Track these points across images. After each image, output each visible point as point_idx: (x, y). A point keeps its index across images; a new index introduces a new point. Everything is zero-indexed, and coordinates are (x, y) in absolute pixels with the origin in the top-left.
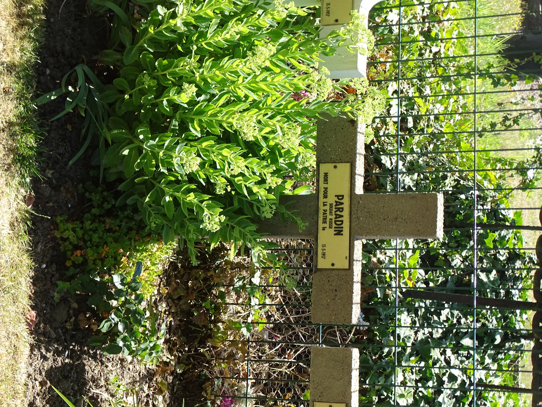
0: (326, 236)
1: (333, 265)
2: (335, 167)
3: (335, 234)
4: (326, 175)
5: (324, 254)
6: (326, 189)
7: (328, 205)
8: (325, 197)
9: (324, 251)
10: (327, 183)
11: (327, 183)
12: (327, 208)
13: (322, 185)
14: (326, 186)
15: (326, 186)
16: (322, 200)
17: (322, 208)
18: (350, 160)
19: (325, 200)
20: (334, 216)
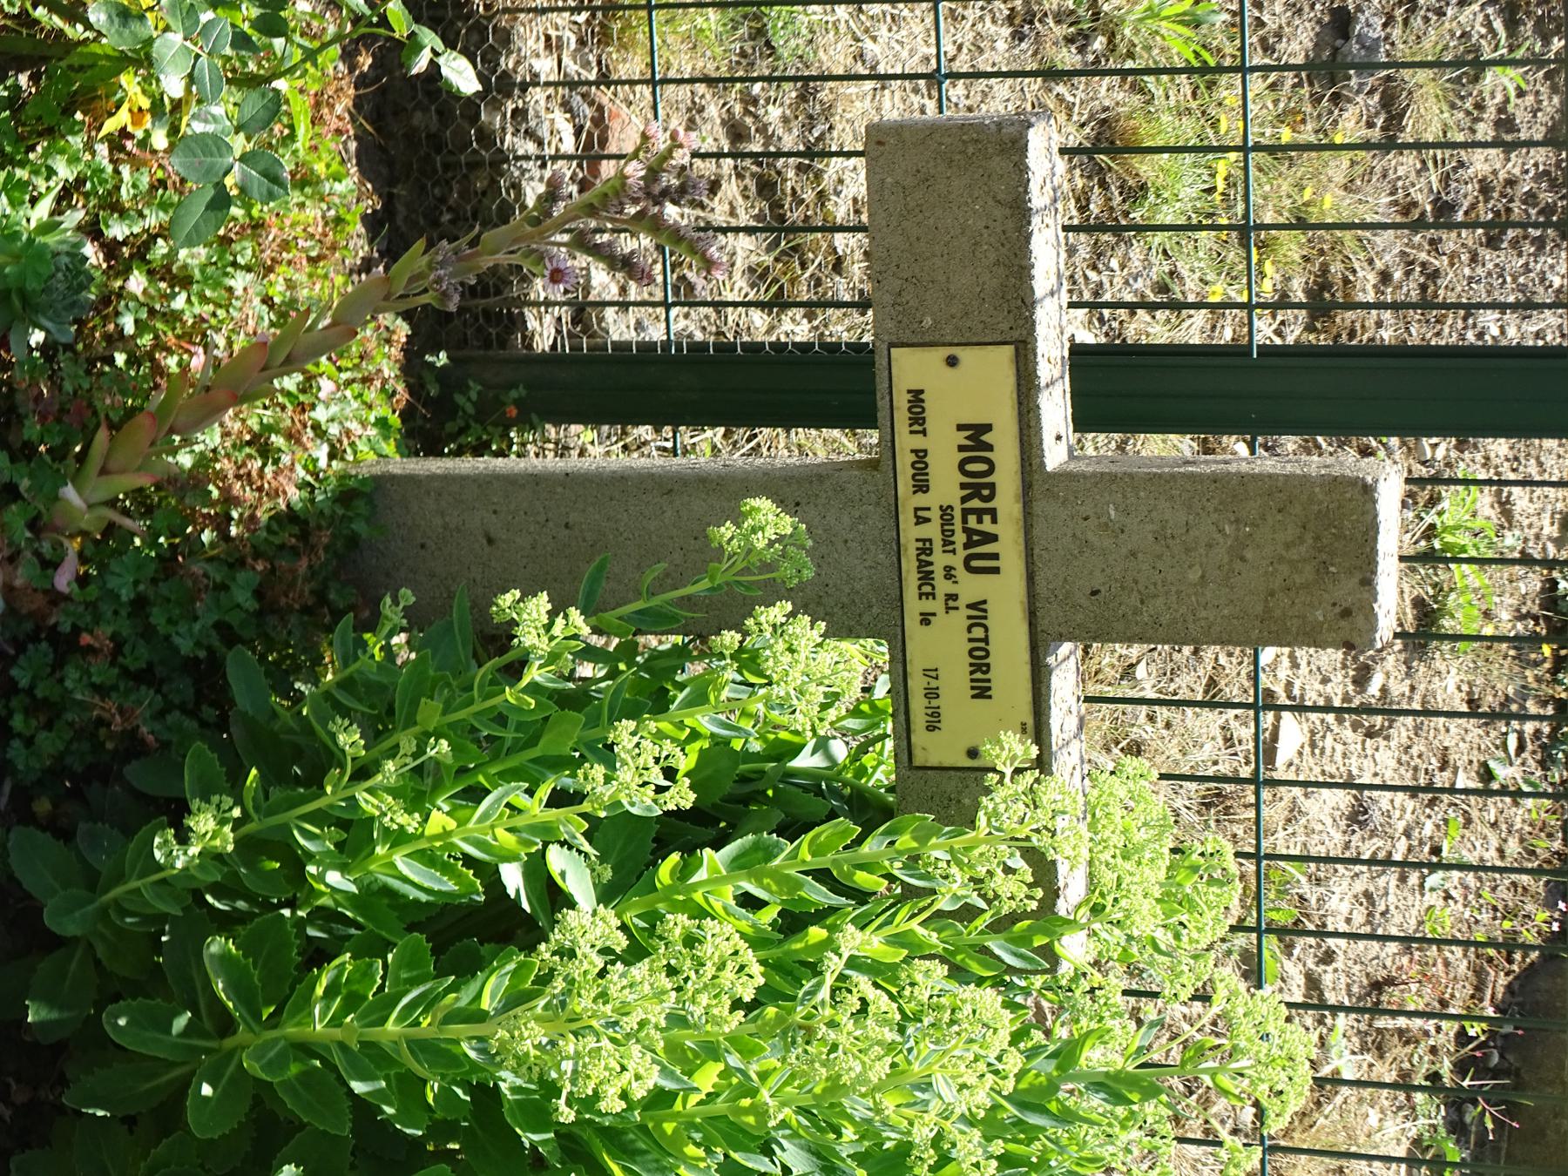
0: (940, 645)
2: (952, 362)
3: (973, 697)
4: (917, 396)
6: (921, 455)
7: (935, 514)
8: (922, 487)
9: (934, 703)
10: (924, 432)
11: (924, 432)
12: (933, 531)
13: (906, 441)
14: (918, 442)
15: (918, 442)
16: (909, 501)
17: (911, 533)
18: (1016, 334)
19: (921, 500)
20: (962, 554)
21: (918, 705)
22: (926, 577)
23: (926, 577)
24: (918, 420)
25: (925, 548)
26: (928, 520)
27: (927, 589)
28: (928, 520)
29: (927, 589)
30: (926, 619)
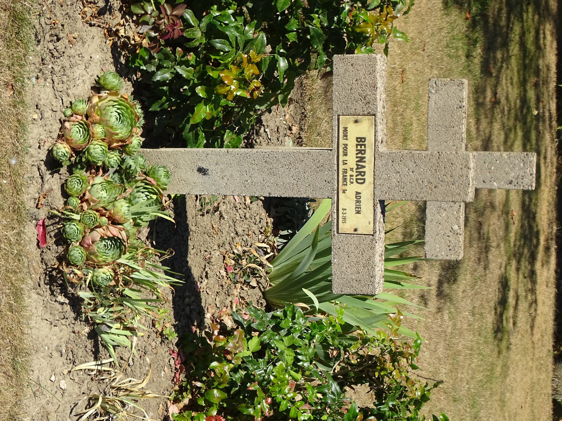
1: (355, 230)
2: (356, 122)
4: (345, 129)
5: (344, 219)
6: (346, 145)
8: (345, 154)
9: (345, 215)
10: (347, 139)
11: (347, 139)
13: (342, 141)
14: (346, 142)
15: (346, 142)
16: (341, 158)
17: (341, 167)
19: (345, 158)
21: (341, 215)
22: (345, 180)
23: (345, 180)
24: (345, 136)
25: (345, 171)
26: (346, 164)
27: (345, 183)
28: (346, 164)
29: (345, 183)
30: (344, 192)
